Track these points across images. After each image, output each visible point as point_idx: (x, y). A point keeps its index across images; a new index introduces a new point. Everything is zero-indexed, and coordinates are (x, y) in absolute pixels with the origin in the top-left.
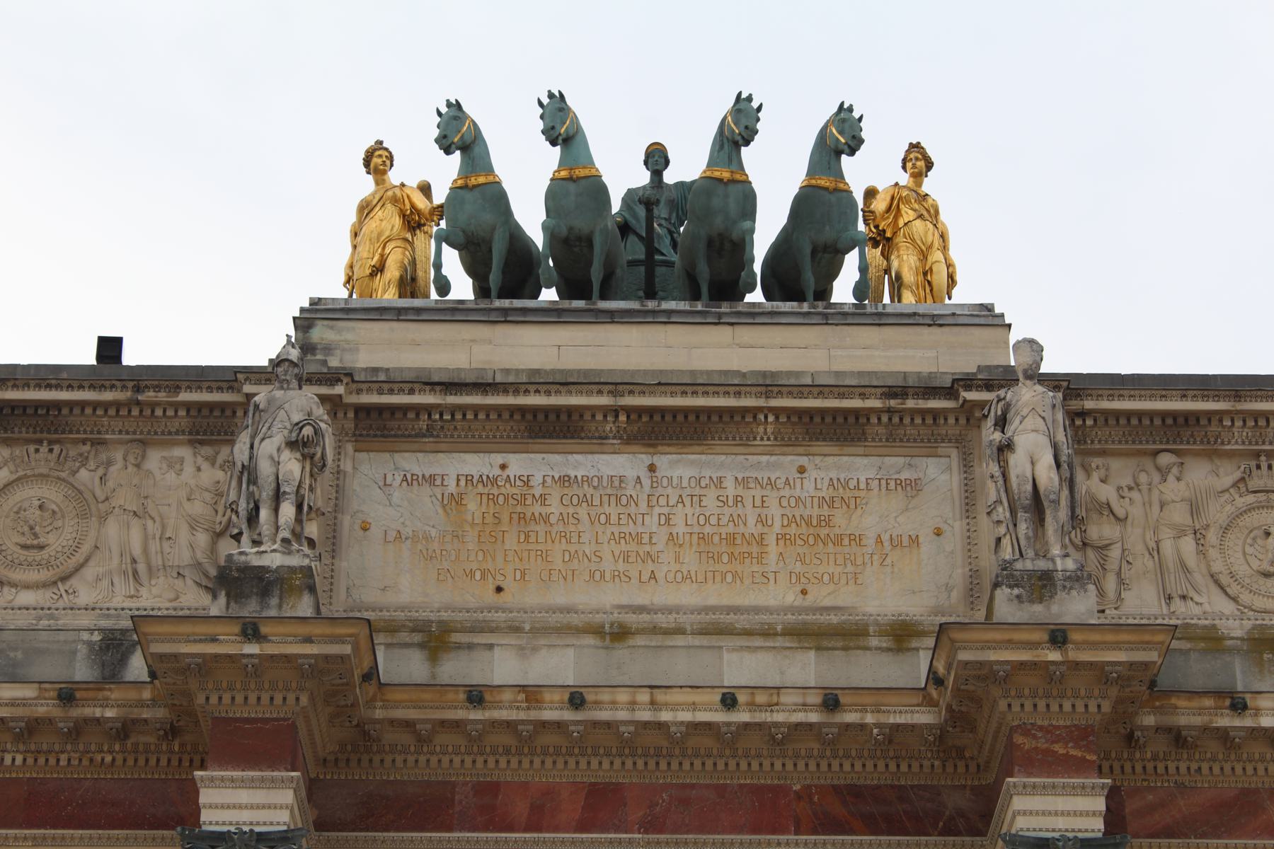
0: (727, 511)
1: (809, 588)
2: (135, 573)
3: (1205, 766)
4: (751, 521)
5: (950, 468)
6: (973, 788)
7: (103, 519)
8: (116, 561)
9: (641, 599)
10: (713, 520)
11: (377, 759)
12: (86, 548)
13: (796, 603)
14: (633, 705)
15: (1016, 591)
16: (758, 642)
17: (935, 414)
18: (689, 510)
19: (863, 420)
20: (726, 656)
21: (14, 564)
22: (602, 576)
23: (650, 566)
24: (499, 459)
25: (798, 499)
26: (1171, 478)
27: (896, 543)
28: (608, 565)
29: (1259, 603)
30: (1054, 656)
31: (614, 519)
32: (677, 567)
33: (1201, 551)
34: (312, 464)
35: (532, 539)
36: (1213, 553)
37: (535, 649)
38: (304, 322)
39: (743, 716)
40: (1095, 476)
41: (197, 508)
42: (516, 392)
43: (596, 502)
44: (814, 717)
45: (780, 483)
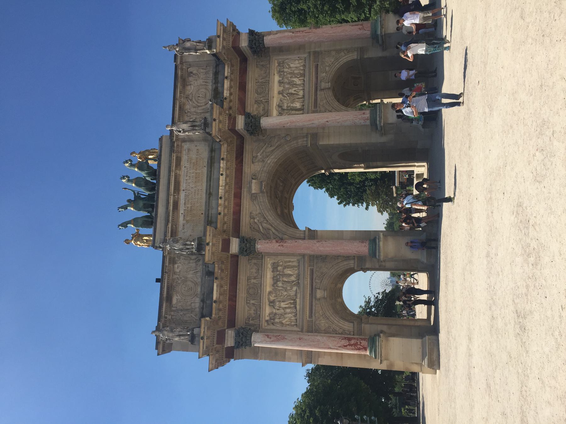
0: (191, 178)
2: (196, 272)
3: (234, 105)
4: (193, 175)
6: (237, 140)
7: (187, 278)
9: (205, 191)
10: (192, 180)
11: (228, 230)
12: (192, 280)
14: (221, 189)
15: (207, 128)
16: (212, 173)
17: (178, 145)
24: (181, 215)
26: (190, 111)
27: (198, 152)
30: (217, 121)
31: (192, 196)
32: (200, 186)
33: (201, 106)
34: (180, 240)
35: (194, 209)
36: (201, 105)
37: (212, 207)
38: (156, 248)
39: (224, 173)
41: (186, 262)
42: (170, 211)
43: (189, 199)
44: (225, 162)
45: (187, 170)
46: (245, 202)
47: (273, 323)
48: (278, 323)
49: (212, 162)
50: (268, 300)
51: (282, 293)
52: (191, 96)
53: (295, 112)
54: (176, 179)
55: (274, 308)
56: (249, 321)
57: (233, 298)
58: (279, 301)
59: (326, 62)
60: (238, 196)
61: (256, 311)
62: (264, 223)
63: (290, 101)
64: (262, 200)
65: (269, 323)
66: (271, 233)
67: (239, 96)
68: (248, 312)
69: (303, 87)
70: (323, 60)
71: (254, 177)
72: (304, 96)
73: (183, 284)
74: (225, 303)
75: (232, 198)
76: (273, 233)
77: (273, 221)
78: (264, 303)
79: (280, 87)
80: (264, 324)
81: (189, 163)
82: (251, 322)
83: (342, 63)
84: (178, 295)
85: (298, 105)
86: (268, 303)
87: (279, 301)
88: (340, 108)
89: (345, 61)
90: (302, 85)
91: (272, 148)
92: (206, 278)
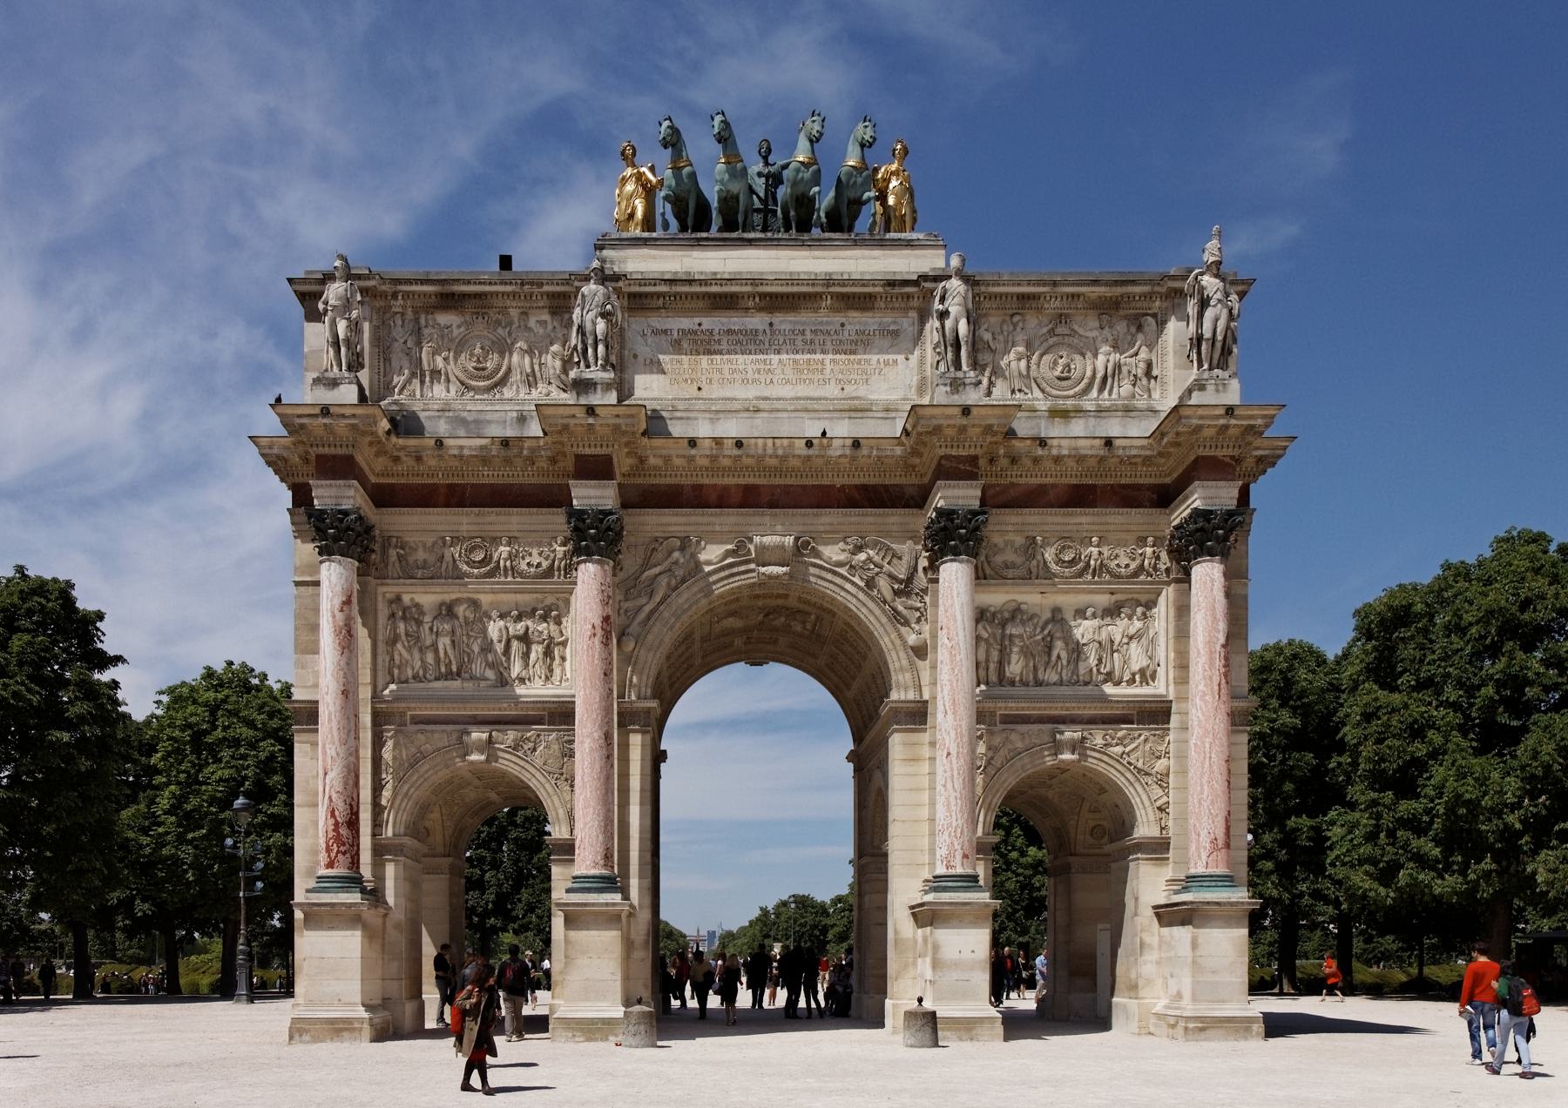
0: (807, 347)
1: (845, 387)
5: (913, 324)
8: (519, 377)
9: (767, 393)
13: (839, 396)
17: (909, 296)
18: (788, 347)
19: (873, 299)
20: (807, 422)
21: (472, 377)
22: (748, 382)
23: (770, 376)
24: (697, 320)
25: (841, 341)
26: (1018, 329)
28: (750, 375)
29: (1055, 392)
33: (1028, 367)
36: (1033, 367)
37: (718, 419)
40: (982, 329)
45: (832, 333)
46: (732, 519)
47: (393, 615)
48: (395, 631)
49: (858, 410)
50: (458, 601)
51: (476, 638)
52: (1068, 332)
53: (996, 659)
54: (805, 298)
55: (435, 618)
56: (396, 547)
57: (456, 496)
58: (453, 632)
59: (1133, 746)
60: (751, 498)
61: (425, 565)
62: (670, 580)
63: (1028, 643)
64: (735, 570)
65: (394, 606)
66: (643, 600)
67: (1054, 486)
68: (420, 545)
69: (1069, 682)
70: (1142, 738)
71: (802, 548)
72: (1041, 685)
73: (493, 342)
74: (440, 476)
75: (742, 481)
76: (640, 608)
77: (674, 608)
78: (446, 588)
79: (1073, 613)
80: (388, 590)
81: (854, 337)
82: (393, 553)
83: (1129, 791)
84: (462, 329)
85: (1015, 667)
86: (448, 601)
87: (453, 632)
88: (998, 791)
89: (1136, 801)
90: (1075, 677)
91: (888, 595)
92: (509, 414)
